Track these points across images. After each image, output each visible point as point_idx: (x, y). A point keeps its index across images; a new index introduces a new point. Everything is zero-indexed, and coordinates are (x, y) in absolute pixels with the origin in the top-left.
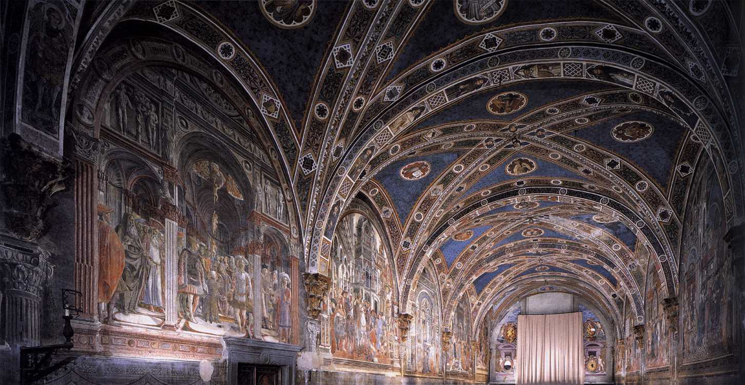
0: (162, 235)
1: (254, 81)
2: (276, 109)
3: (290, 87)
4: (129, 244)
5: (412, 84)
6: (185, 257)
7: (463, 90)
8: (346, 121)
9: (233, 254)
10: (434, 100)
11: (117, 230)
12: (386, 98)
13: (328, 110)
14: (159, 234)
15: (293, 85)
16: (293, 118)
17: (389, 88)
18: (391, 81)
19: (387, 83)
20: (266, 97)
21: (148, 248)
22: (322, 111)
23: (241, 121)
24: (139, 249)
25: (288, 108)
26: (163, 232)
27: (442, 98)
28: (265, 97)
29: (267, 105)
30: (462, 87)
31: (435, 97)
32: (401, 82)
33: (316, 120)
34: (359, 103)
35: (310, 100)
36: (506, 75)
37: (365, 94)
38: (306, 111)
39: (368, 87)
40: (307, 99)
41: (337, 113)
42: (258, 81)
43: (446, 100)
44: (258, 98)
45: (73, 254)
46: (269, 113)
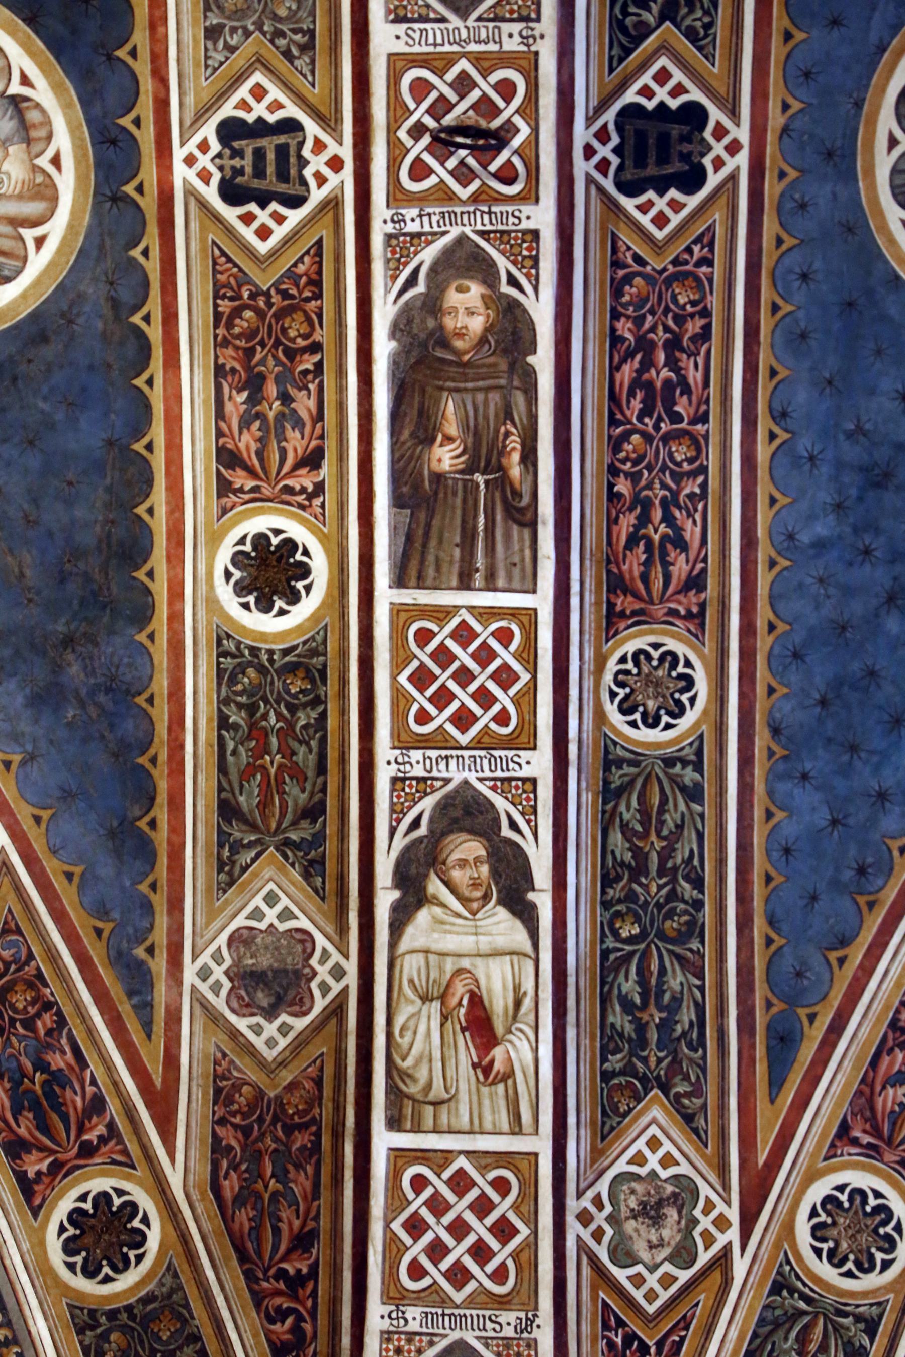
5: (313, 812)
7: (483, 455)
10: (443, 698)
12: (269, 1035)
17: (203, 970)
18: (160, 935)
19: (159, 965)
27: (464, 635)
30: (445, 458)
31: (422, 678)
32: (228, 872)
34: (103, 1235)
36: (463, 84)
37: (87, 1151)
39: (59, 1107)
43: (514, 613)
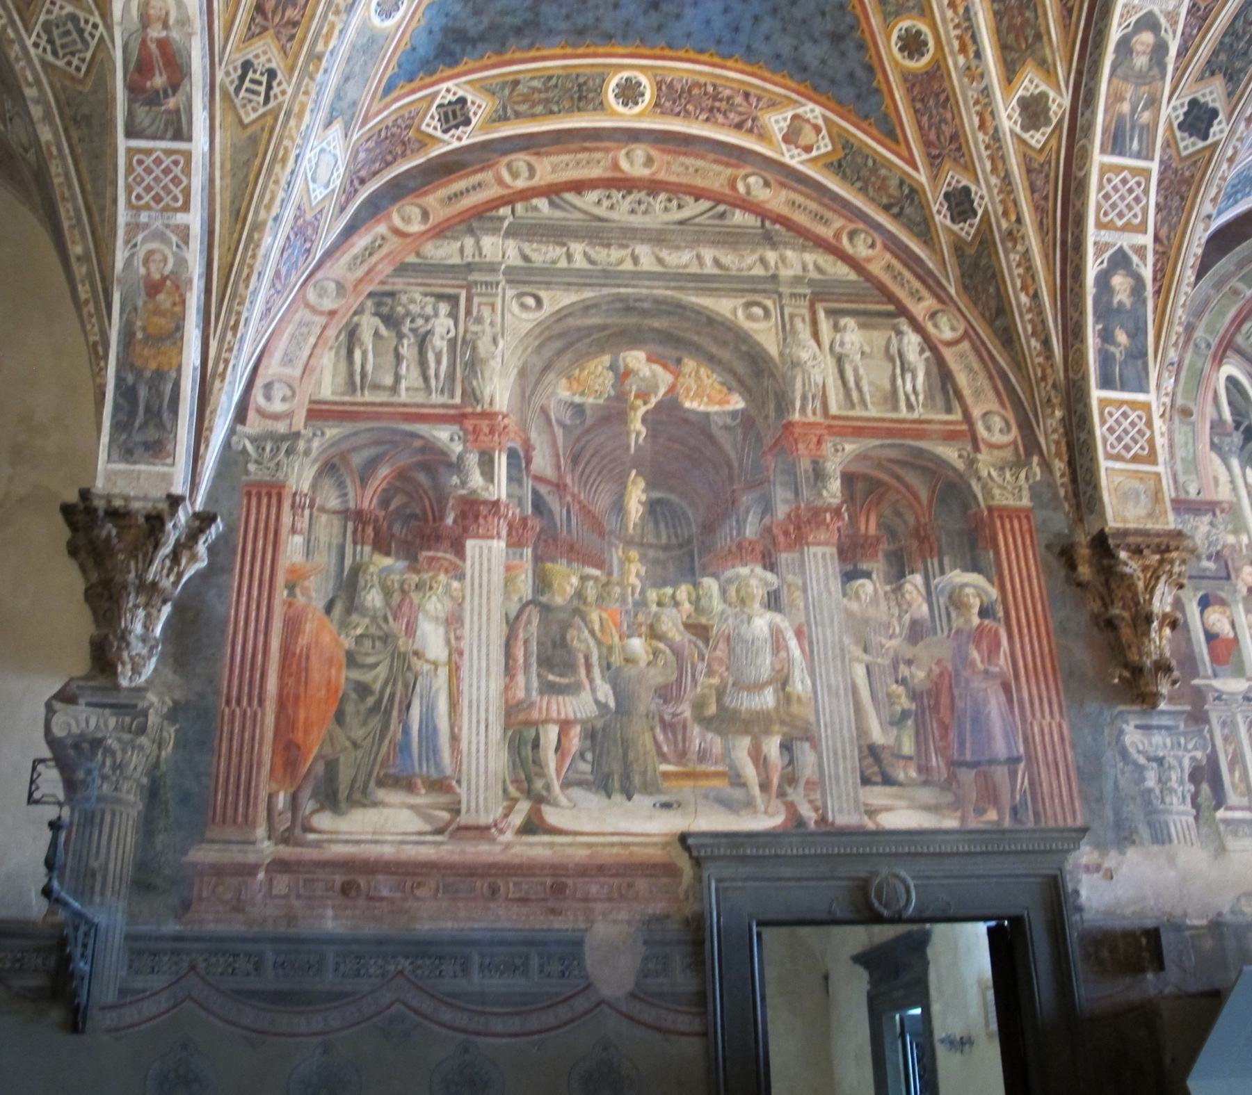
0: (455, 584)
1: (732, 106)
2: (817, 129)
3: (812, 54)
4: (359, 631)
6: (529, 622)
8: (996, 13)
9: (711, 570)
11: (329, 609)
13: (924, 28)
14: (448, 586)
15: (815, 41)
16: (862, 118)
20: (777, 122)
21: (411, 629)
22: (912, 44)
23: (722, 216)
24: (386, 639)
25: (839, 105)
26: (461, 577)
28: (777, 122)
29: (790, 137)
33: (915, 76)
35: (870, 44)
38: (880, 76)
40: (861, 46)
41: (950, 14)
42: (739, 99)
44: (763, 136)
45: (217, 693)
46: (808, 149)
